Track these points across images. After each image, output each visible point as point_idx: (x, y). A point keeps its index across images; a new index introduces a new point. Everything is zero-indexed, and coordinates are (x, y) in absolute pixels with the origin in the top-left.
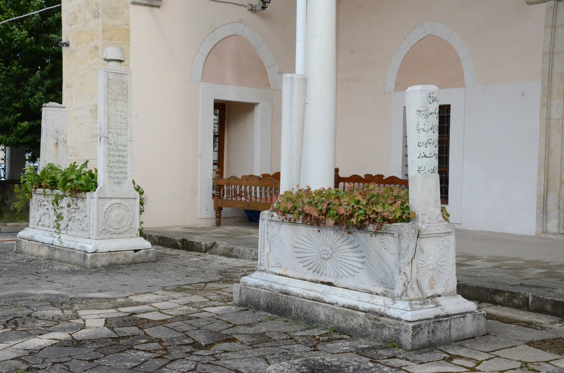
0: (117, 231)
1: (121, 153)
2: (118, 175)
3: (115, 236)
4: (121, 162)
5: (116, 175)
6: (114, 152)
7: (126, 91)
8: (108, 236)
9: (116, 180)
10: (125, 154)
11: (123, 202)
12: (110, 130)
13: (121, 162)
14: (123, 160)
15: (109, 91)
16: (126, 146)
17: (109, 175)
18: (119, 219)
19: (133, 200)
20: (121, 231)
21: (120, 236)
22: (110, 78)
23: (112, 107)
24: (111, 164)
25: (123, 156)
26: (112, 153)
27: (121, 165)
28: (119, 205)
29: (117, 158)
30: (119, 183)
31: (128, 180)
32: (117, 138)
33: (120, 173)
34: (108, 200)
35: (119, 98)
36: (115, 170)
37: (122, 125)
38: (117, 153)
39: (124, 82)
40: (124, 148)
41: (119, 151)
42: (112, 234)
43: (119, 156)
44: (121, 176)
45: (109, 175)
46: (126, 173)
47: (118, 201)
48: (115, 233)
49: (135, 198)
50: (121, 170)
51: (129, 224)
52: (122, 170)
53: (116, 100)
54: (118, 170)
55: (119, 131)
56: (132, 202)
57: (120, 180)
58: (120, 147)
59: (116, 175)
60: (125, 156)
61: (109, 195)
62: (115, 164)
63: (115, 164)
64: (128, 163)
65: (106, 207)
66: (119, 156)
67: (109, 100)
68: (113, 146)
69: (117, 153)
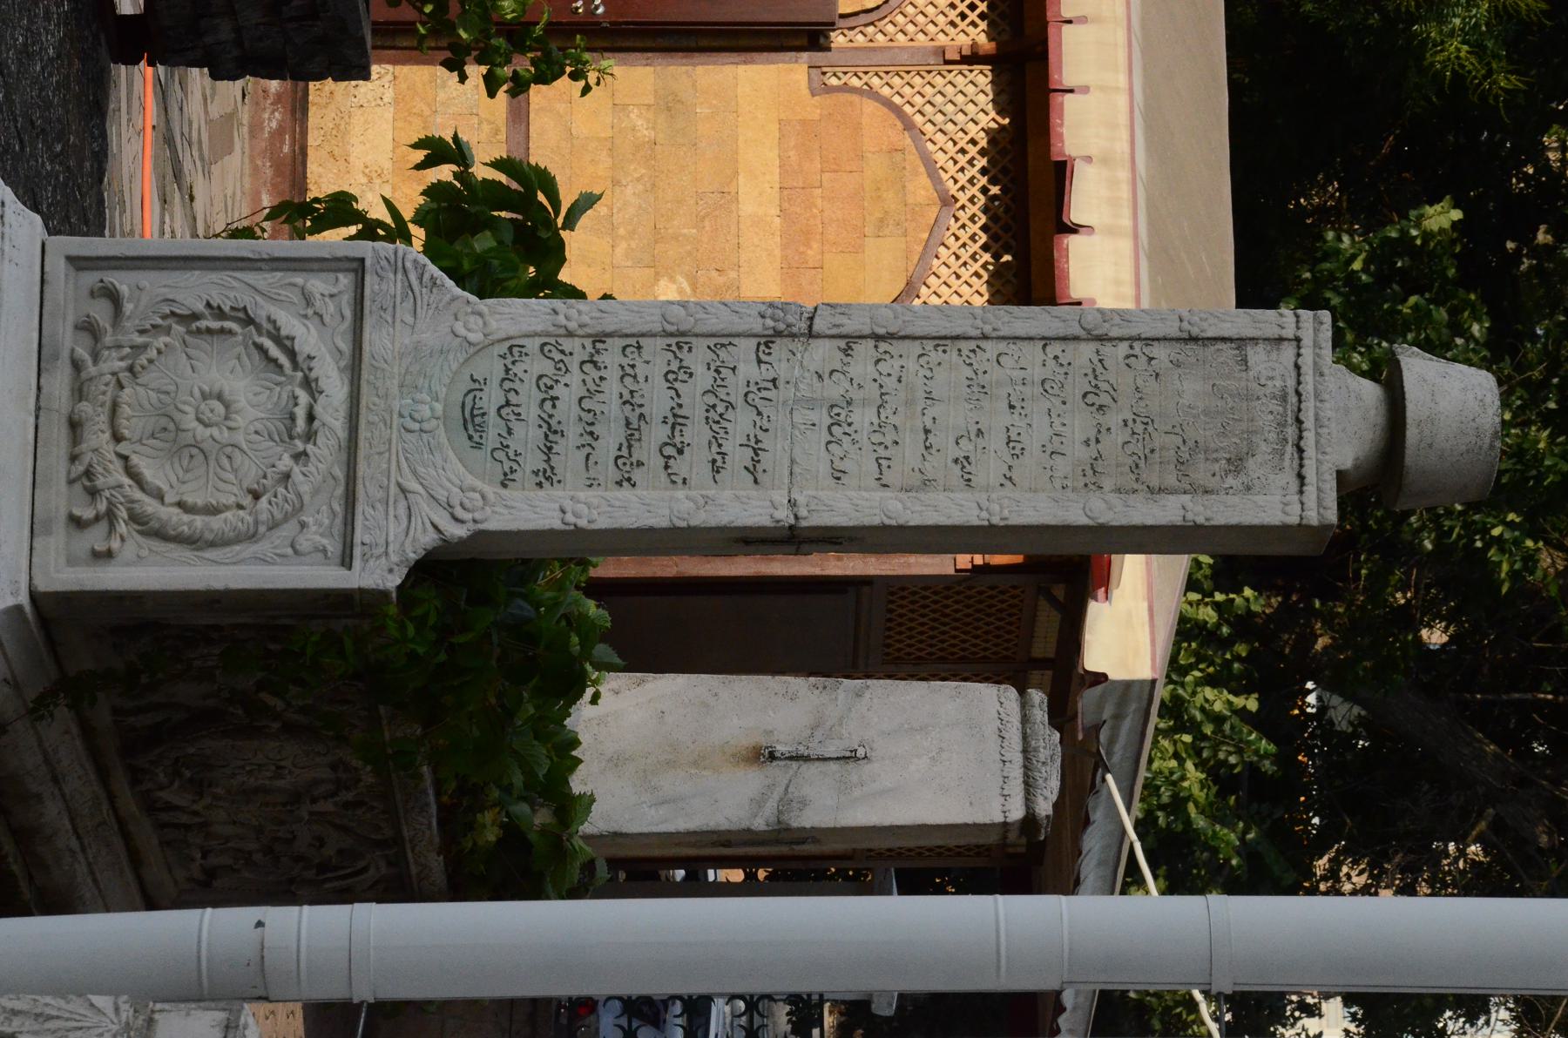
0: (95, 416)
1: (696, 433)
2: (531, 412)
3: (59, 383)
5: (528, 400)
6: (704, 379)
7: (1171, 480)
8: (66, 338)
9: (492, 398)
10: (695, 463)
11: (326, 451)
12: (864, 349)
15: (1159, 351)
17: (533, 345)
18: (190, 422)
19: (333, 547)
20: (97, 437)
21: (57, 434)
22: (1256, 355)
23: (1038, 373)
24: (611, 357)
25: (674, 449)
26: (699, 369)
27: (611, 438)
28: (298, 430)
29: (658, 401)
30: (471, 420)
31: (490, 491)
32: (811, 403)
33: (551, 432)
34: (345, 347)
35: (1114, 419)
36: (569, 393)
38: (695, 407)
39: (1236, 464)
40: (738, 457)
42: (77, 365)
43: (676, 420)
44: (528, 436)
46: (546, 477)
48: (79, 392)
49: (346, 561)
50: (573, 432)
51: (150, 506)
52: (568, 456)
53: (1095, 399)
55: (863, 418)
56: (319, 528)
58: (742, 422)
59: (528, 400)
60: (680, 466)
61: (377, 339)
62: (613, 388)
63: (613, 388)
64: (626, 493)
65: (290, 324)
66: (676, 420)
67: (1087, 350)
68: (748, 370)
69: (695, 407)
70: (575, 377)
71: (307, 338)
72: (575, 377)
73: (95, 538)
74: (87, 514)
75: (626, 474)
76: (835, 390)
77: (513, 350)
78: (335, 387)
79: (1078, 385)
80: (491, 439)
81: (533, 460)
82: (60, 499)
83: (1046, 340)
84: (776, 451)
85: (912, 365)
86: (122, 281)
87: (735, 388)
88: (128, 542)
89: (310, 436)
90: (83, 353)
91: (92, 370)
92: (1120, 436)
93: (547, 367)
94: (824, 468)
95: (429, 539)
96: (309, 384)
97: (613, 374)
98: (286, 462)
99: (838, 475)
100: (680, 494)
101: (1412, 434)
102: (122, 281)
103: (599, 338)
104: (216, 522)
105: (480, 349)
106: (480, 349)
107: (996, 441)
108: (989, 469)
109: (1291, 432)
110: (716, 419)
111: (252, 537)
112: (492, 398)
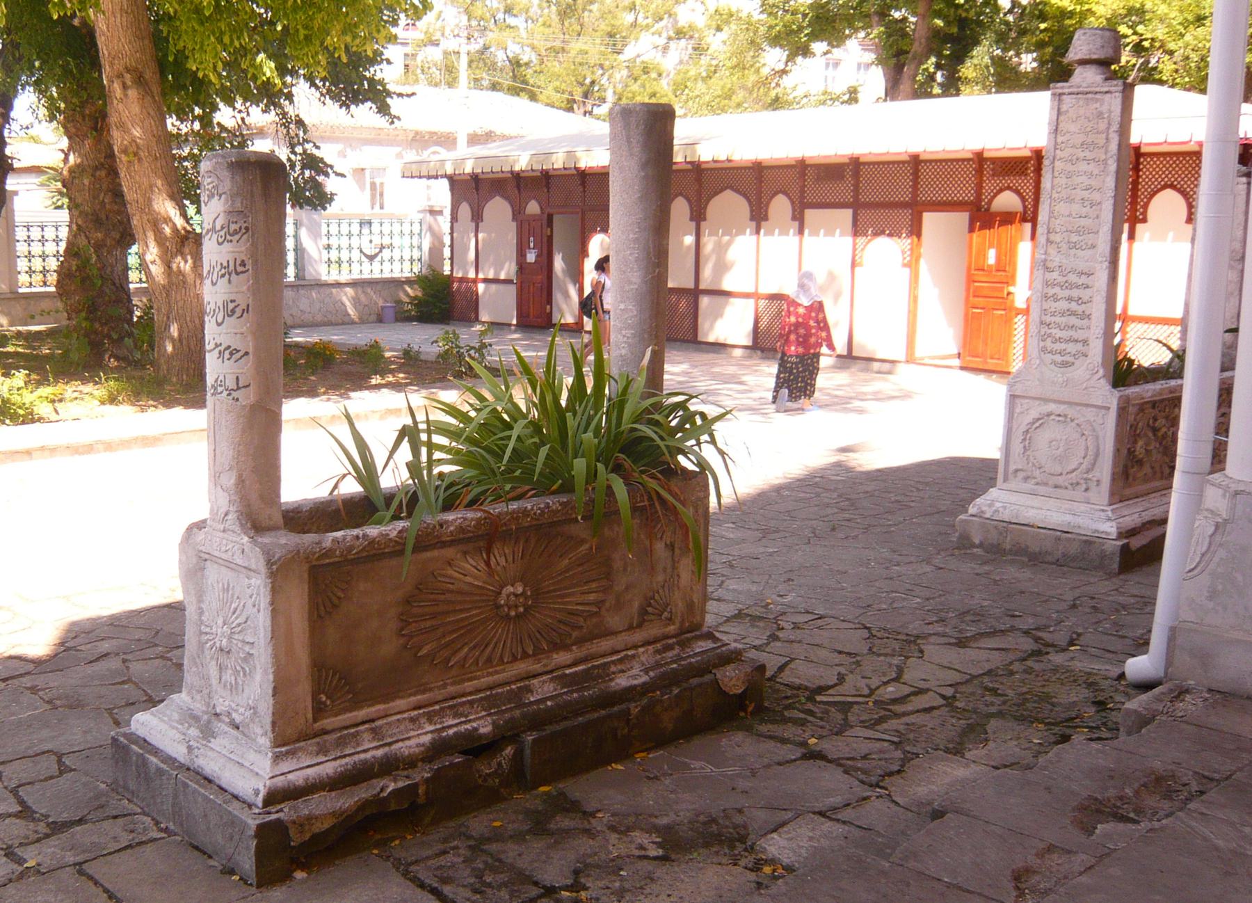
1: (1075, 293)
2: (1063, 346)
4: (1074, 313)
5: (1058, 346)
8: (1029, 486)
9: (1058, 358)
10: (1085, 295)
11: (1071, 412)
12: (1052, 237)
13: (1074, 313)
14: (1080, 309)
16: (1089, 275)
17: (1042, 344)
18: (1058, 452)
19: (1103, 412)
20: (1060, 480)
24: (1048, 319)
25: (1079, 301)
27: (1073, 320)
29: (1063, 305)
30: (1065, 365)
34: (1037, 402)
36: (1058, 333)
37: (1083, 222)
38: (1066, 293)
40: (1083, 280)
41: (1072, 286)
43: (1070, 299)
44: (1071, 348)
45: (1042, 344)
46: (1085, 342)
47: (1061, 409)
48: (1046, 484)
50: (1071, 333)
51: (1084, 466)
52: (1080, 335)
54: (1064, 334)
55: (1074, 238)
57: (1067, 358)
58: (1073, 278)
59: (1058, 346)
60: (1085, 299)
62: (1058, 319)
63: (1058, 319)
64: (1093, 317)
65: (1029, 419)
66: (1070, 299)
67: (1057, 163)
68: (1055, 275)
69: (1066, 293)
70: (1054, 331)
71: (1034, 414)
72: (1054, 331)
73: (1092, 485)
74: (1084, 486)
75: (1086, 316)
76: (1064, 246)
77: (1044, 350)
78: (1052, 407)
79: (1070, 167)
80: (1071, 359)
81: (1079, 346)
82: (1078, 494)
83: (1053, 177)
84: (1082, 266)
85: (1058, 222)
86: (1012, 467)
87: (1061, 279)
88: (1095, 474)
89: (1066, 416)
90: (1034, 481)
91: (1039, 480)
92: (1087, 153)
93: (1049, 340)
94: (1090, 252)
95: (1103, 381)
96: (1049, 415)
97: (1053, 319)
98: (1073, 424)
99: (1093, 247)
100: (1094, 299)
101: (1095, 57)
102: (1012, 467)
103: (1042, 323)
104: (1091, 448)
105: (1042, 360)
106: (1042, 360)
107: (1086, 194)
108: (1096, 196)
109: (1090, 96)
110: (1072, 286)
111: (1097, 437)
112: (1058, 358)
